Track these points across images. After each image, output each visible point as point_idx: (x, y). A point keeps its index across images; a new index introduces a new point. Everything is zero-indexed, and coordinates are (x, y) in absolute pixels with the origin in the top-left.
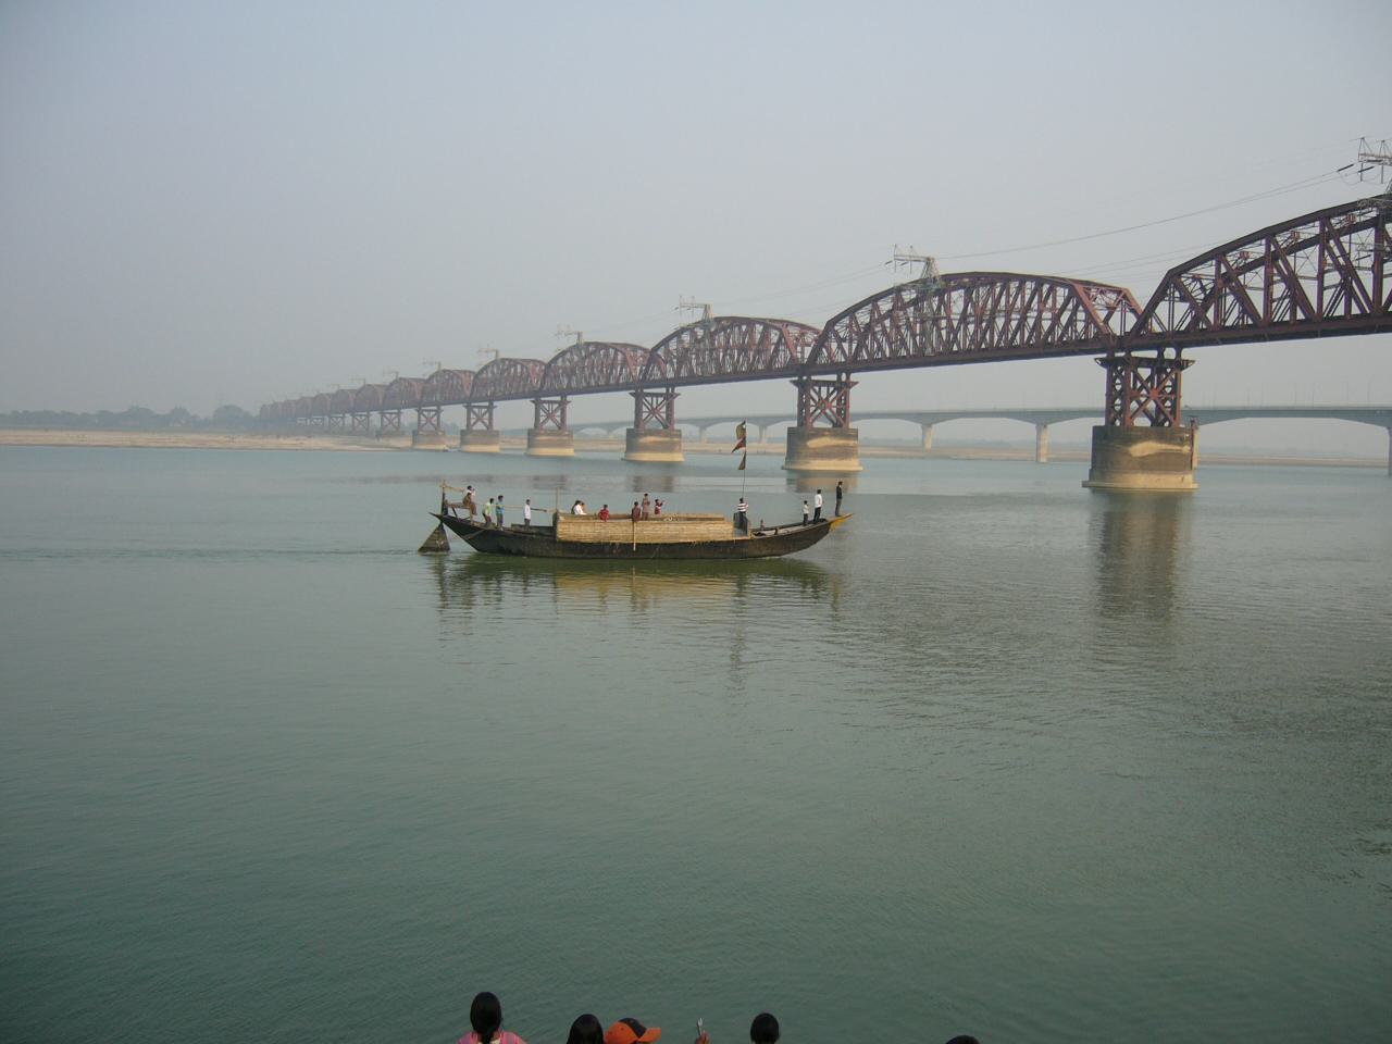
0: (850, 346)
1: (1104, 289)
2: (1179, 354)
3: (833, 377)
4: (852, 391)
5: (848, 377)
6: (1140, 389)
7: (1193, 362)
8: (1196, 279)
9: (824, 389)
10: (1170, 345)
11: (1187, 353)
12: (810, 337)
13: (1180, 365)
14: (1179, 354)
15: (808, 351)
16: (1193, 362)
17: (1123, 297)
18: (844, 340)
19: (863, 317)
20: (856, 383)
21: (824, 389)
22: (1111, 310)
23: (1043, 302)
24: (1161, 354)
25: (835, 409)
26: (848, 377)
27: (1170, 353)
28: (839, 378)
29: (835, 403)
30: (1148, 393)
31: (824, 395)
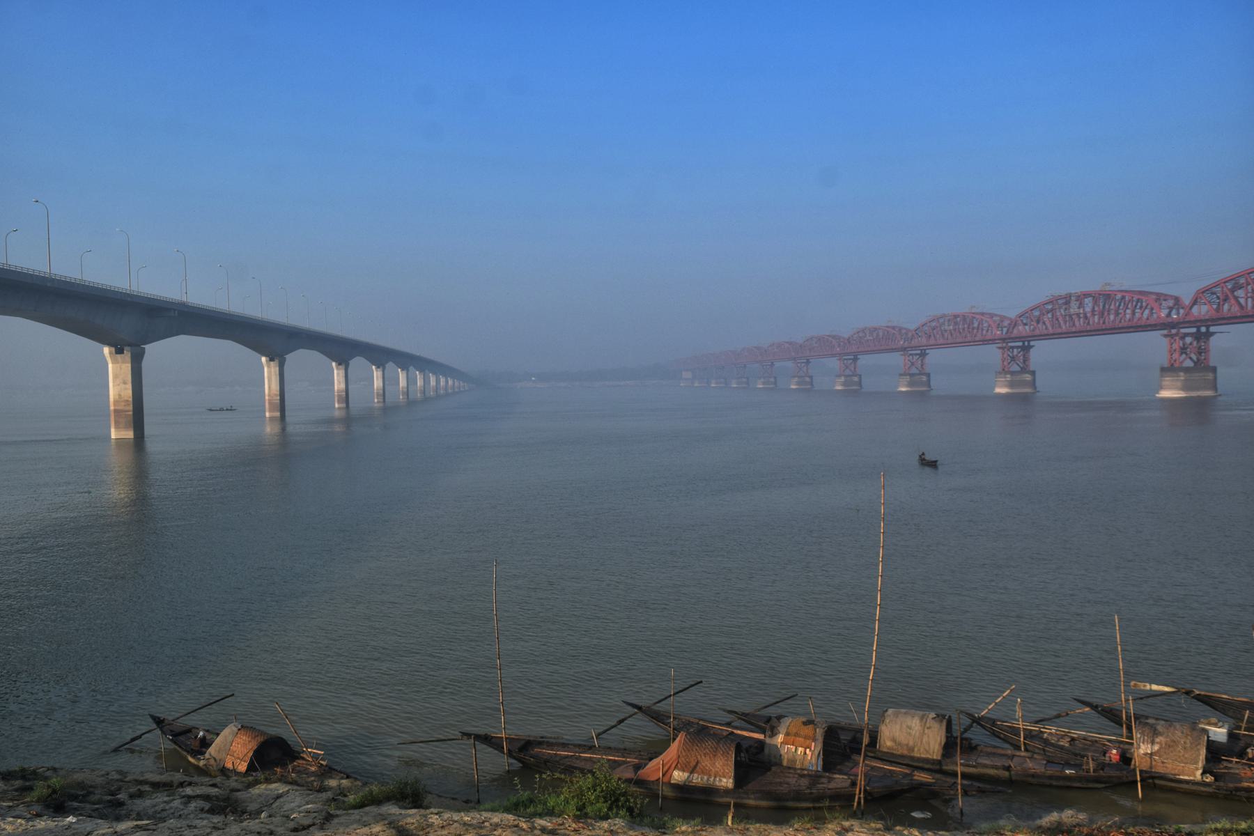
0: (1030, 328)
1: (1166, 297)
3: (1020, 344)
5: (1029, 343)
8: (1213, 293)
9: (1015, 350)
10: (1203, 326)
12: (1006, 323)
15: (1005, 330)
17: (1177, 300)
18: (1025, 324)
19: (1037, 313)
21: (1015, 350)
22: (1171, 309)
24: (1198, 330)
25: (1022, 361)
26: (1029, 343)
27: (1203, 329)
28: (1024, 344)
29: (1022, 358)
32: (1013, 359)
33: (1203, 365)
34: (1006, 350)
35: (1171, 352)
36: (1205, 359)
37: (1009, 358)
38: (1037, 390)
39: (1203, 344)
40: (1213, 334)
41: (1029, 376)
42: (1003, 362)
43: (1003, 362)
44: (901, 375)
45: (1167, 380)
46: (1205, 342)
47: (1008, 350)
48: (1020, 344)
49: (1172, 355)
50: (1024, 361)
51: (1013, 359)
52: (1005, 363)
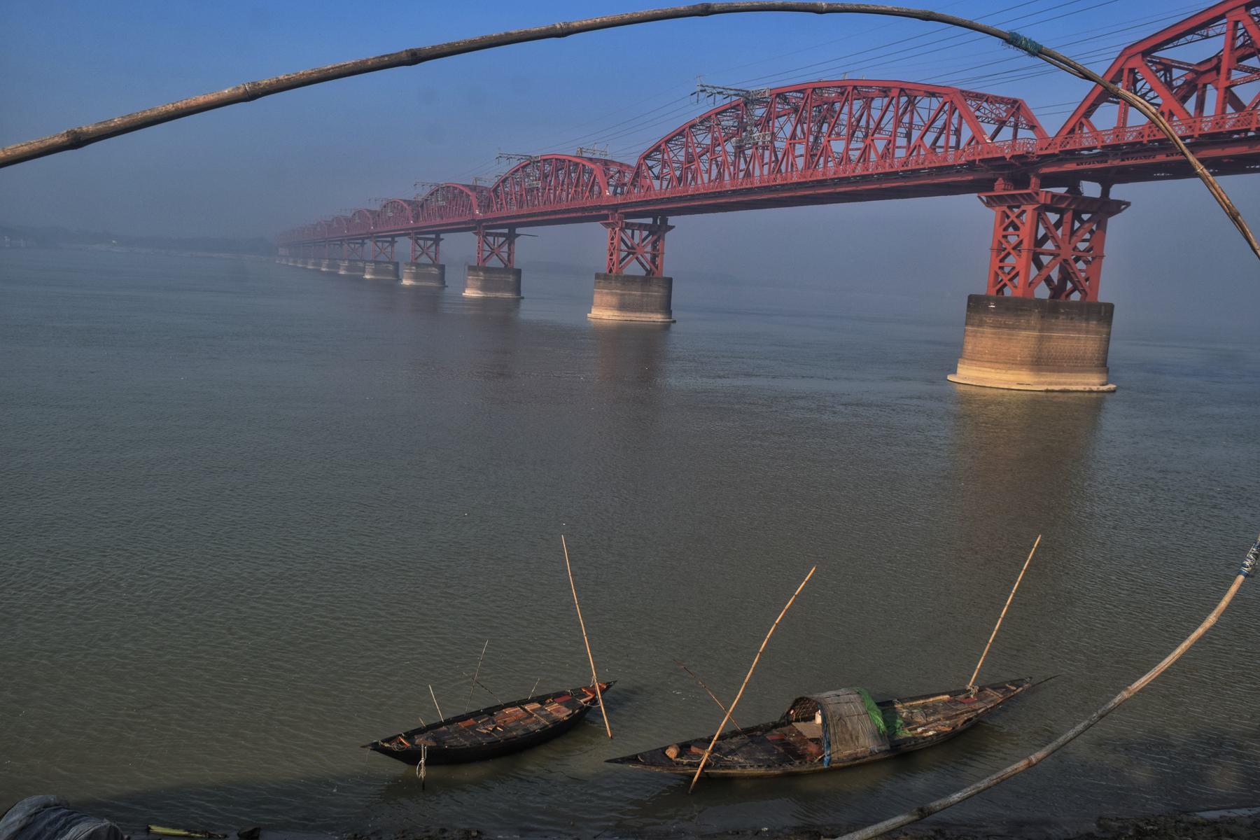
2: (1105, 192)
3: (649, 221)
4: (668, 235)
6: (1045, 238)
7: (1128, 204)
9: (637, 233)
11: (1118, 192)
13: (1106, 208)
14: (1105, 192)
16: (1128, 204)
20: (674, 227)
21: (637, 233)
23: (898, 121)
25: (648, 256)
27: (1091, 189)
28: (655, 221)
30: (1058, 247)
31: (637, 240)
32: (632, 250)
33: (1076, 296)
34: (617, 229)
35: (1001, 252)
36: (1087, 280)
37: (624, 247)
38: (674, 317)
39: (1087, 236)
40: (1118, 207)
41: (661, 290)
42: (611, 255)
43: (611, 255)
44: (472, 268)
45: (983, 339)
46: (1091, 232)
47: (622, 229)
48: (649, 221)
49: (1002, 260)
50: (654, 257)
51: (632, 250)
52: (614, 257)
